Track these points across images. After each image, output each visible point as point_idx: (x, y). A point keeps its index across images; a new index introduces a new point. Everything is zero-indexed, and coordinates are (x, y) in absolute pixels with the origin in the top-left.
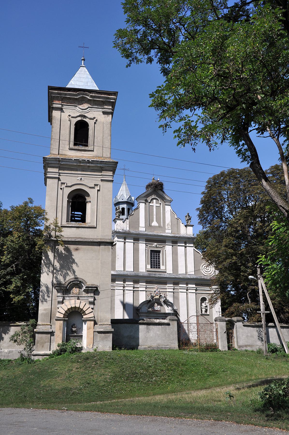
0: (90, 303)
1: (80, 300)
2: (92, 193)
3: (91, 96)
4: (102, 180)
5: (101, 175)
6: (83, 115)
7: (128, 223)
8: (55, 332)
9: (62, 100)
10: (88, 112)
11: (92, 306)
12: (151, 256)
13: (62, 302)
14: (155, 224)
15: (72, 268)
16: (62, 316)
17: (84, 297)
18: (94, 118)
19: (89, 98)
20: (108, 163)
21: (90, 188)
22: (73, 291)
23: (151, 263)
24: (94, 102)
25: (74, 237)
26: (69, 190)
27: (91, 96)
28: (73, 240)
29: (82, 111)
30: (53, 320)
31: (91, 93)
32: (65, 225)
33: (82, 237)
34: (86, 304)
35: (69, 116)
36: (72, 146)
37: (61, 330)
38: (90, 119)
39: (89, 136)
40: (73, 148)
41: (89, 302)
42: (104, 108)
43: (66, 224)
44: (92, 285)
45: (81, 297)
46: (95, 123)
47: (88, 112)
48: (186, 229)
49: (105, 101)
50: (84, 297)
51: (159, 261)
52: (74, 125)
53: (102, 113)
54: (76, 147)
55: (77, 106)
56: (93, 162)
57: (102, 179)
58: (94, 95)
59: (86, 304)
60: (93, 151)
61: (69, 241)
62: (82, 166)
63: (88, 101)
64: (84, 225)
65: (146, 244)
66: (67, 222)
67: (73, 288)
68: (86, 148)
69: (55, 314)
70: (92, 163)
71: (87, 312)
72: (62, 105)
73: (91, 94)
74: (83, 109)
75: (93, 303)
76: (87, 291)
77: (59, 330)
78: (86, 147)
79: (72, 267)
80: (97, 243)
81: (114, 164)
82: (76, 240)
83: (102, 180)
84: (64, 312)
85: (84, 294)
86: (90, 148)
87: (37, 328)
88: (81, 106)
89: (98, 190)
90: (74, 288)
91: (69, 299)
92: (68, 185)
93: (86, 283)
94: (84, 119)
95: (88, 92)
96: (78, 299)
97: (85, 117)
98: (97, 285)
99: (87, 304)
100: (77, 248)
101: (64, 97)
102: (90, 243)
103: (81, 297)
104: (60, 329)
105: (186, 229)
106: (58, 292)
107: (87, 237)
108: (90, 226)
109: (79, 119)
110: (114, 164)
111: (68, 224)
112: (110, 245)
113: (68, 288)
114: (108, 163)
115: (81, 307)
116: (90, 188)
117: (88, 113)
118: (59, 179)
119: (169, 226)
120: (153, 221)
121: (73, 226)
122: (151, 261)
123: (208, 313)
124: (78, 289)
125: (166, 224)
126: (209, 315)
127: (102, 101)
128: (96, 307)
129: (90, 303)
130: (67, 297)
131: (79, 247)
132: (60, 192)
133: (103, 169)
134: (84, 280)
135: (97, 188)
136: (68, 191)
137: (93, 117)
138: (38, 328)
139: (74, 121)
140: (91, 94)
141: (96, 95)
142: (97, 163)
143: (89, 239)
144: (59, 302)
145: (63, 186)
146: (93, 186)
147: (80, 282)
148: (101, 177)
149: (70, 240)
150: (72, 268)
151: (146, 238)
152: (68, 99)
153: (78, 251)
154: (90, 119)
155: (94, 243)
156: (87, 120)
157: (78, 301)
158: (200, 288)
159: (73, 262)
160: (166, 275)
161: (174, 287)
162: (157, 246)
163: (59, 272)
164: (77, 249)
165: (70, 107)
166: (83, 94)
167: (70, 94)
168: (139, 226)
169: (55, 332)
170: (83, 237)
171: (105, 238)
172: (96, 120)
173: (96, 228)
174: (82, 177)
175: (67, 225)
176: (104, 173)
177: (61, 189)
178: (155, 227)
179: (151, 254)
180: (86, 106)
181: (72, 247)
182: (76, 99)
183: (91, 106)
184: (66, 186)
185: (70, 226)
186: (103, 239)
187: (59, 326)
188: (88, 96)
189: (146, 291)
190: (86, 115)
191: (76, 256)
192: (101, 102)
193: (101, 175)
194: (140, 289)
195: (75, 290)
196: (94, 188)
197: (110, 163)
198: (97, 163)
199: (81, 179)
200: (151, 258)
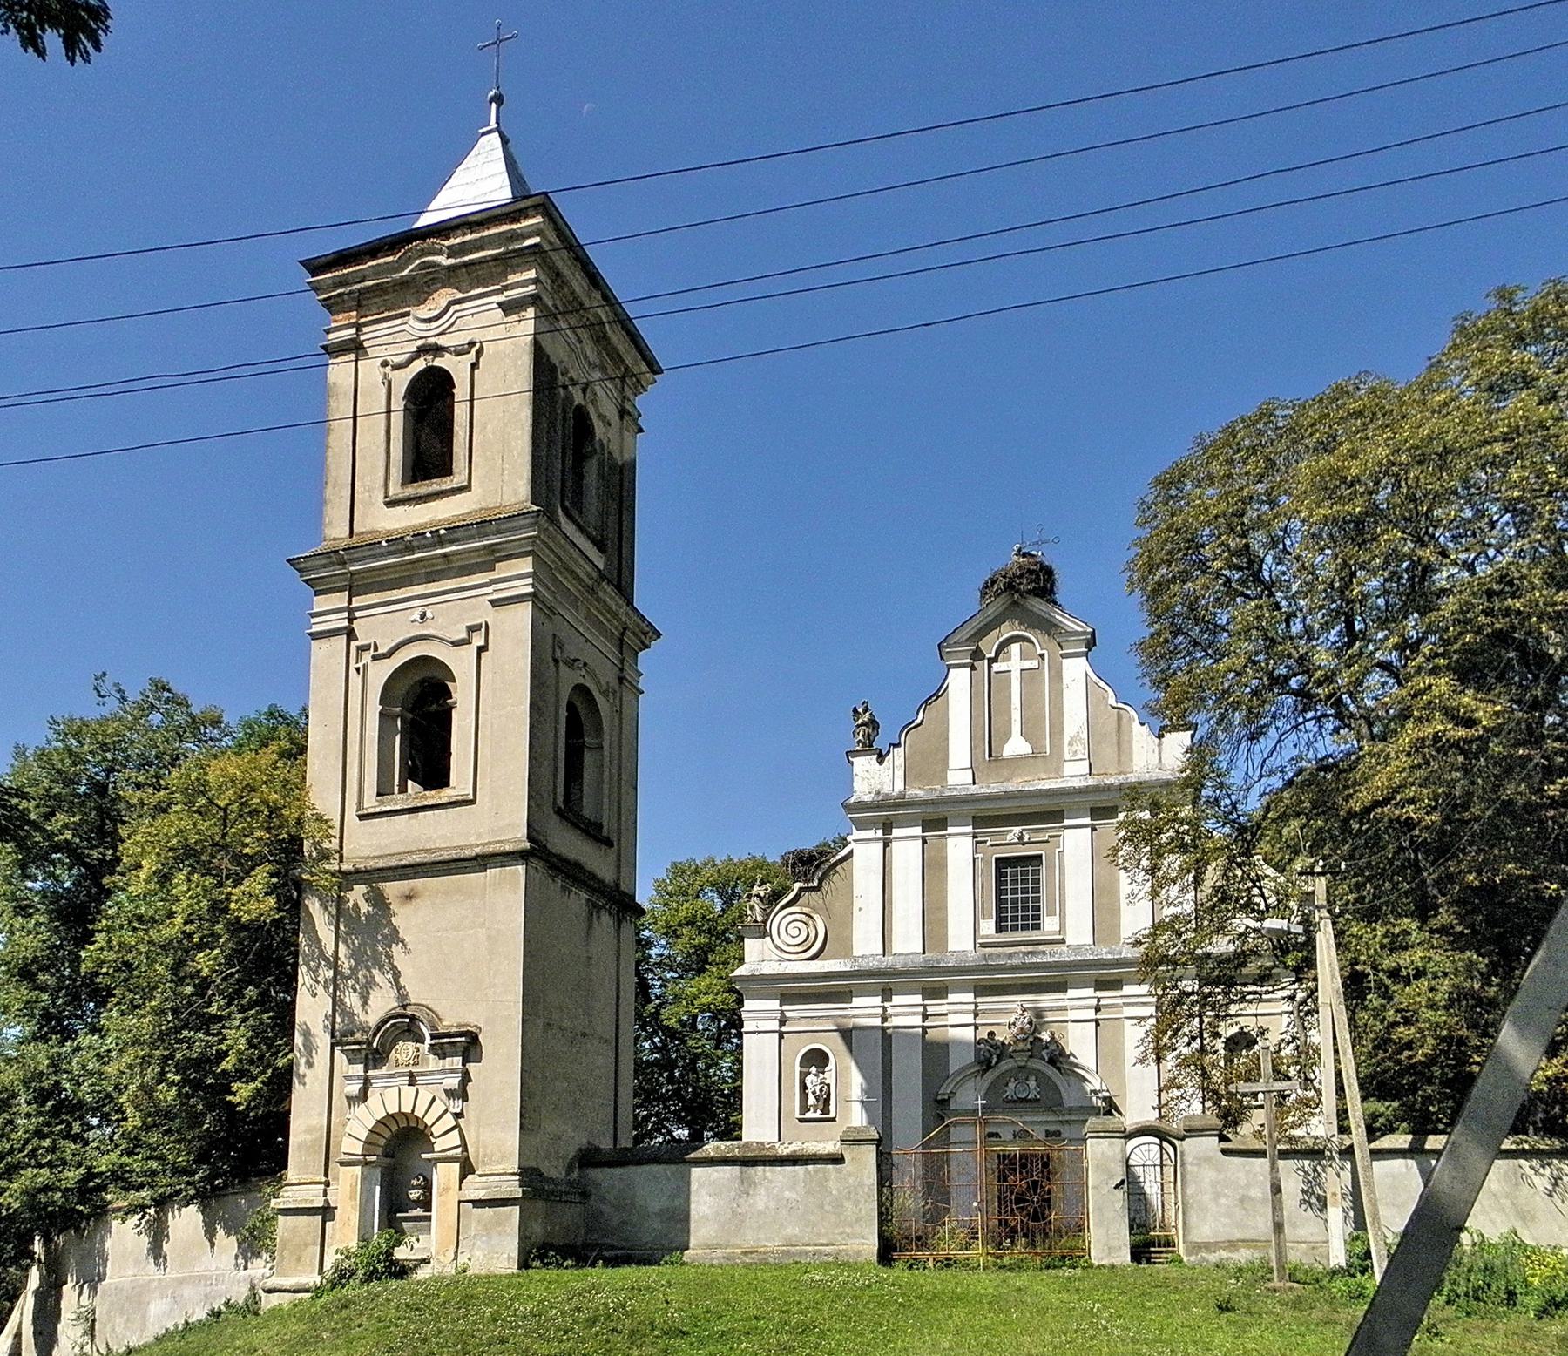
1: (414, 1088)
2: (460, 663)
3: (453, 252)
4: (495, 603)
5: (493, 582)
7: (900, 761)
11: (456, 1106)
13: (363, 1096)
14: (1016, 746)
16: (358, 1148)
17: (432, 1073)
19: (443, 260)
21: (455, 644)
27: (453, 252)
31: (448, 238)
32: (372, 811)
34: (434, 1099)
36: (395, 490)
39: (456, 427)
42: (506, 288)
44: (459, 1025)
45: (422, 1074)
46: (474, 366)
48: (1160, 745)
49: (504, 254)
52: (404, 398)
54: (412, 490)
55: (408, 314)
56: (455, 535)
57: (495, 596)
58: (458, 240)
59: (434, 1099)
60: (466, 488)
62: (426, 563)
63: (450, 277)
66: (379, 794)
68: (446, 483)
70: (452, 542)
72: (359, 327)
74: (429, 321)
76: (440, 1051)
81: (531, 525)
82: (403, 862)
83: (495, 603)
84: (363, 1135)
85: (433, 1063)
86: (458, 479)
88: (425, 311)
90: (401, 1043)
92: (380, 651)
94: (438, 362)
96: (412, 1082)
97: (437, 350)
99: (437, 1100)
103: (422, 1074)
105: (1160, 745)
106: (351, 1062)
108: (454, 799)
109: (419, 365)
110: (531, 525)
111: (382, 803)
113: (375, 1045)
115: (419, 1113)
116: (455, 644)
118: (350, 634)
119: (1081, 748)
120: (1007, 735)
121: (398, 807)
124: (411, 1046)
125: (1067, 739)
127: (495, 258)
130: (376, 1077)
132: (355, 680)
135: (478, 640)
136: (380, 673)
139: (402, 379)
141: (468, 237)
144: (351, 1100)
145: (367, 657)
146: (464, 635)
148: (490, 590)
149: (381, 864)
154: (459, 353)
156: (444, 362)
164: (409, 897)
165: (385, 325)
166: (424, 253)
172: (479, 353)
173: (473, 802)
175: (378, 810)
176: (504, 569)
177: (358, 670)
178: (1017, 760)
180: (442, 297)
181: (392, 889)
182: (404, 284)
183: (461, 295)
184: (374, 658)
185: (388, 808)
188: (440, 253)
190: (442, 341)
191: (402, 918)
193: (493, 582)
195: (404, 1050)
196: (466, 642)
199: (423, 616)
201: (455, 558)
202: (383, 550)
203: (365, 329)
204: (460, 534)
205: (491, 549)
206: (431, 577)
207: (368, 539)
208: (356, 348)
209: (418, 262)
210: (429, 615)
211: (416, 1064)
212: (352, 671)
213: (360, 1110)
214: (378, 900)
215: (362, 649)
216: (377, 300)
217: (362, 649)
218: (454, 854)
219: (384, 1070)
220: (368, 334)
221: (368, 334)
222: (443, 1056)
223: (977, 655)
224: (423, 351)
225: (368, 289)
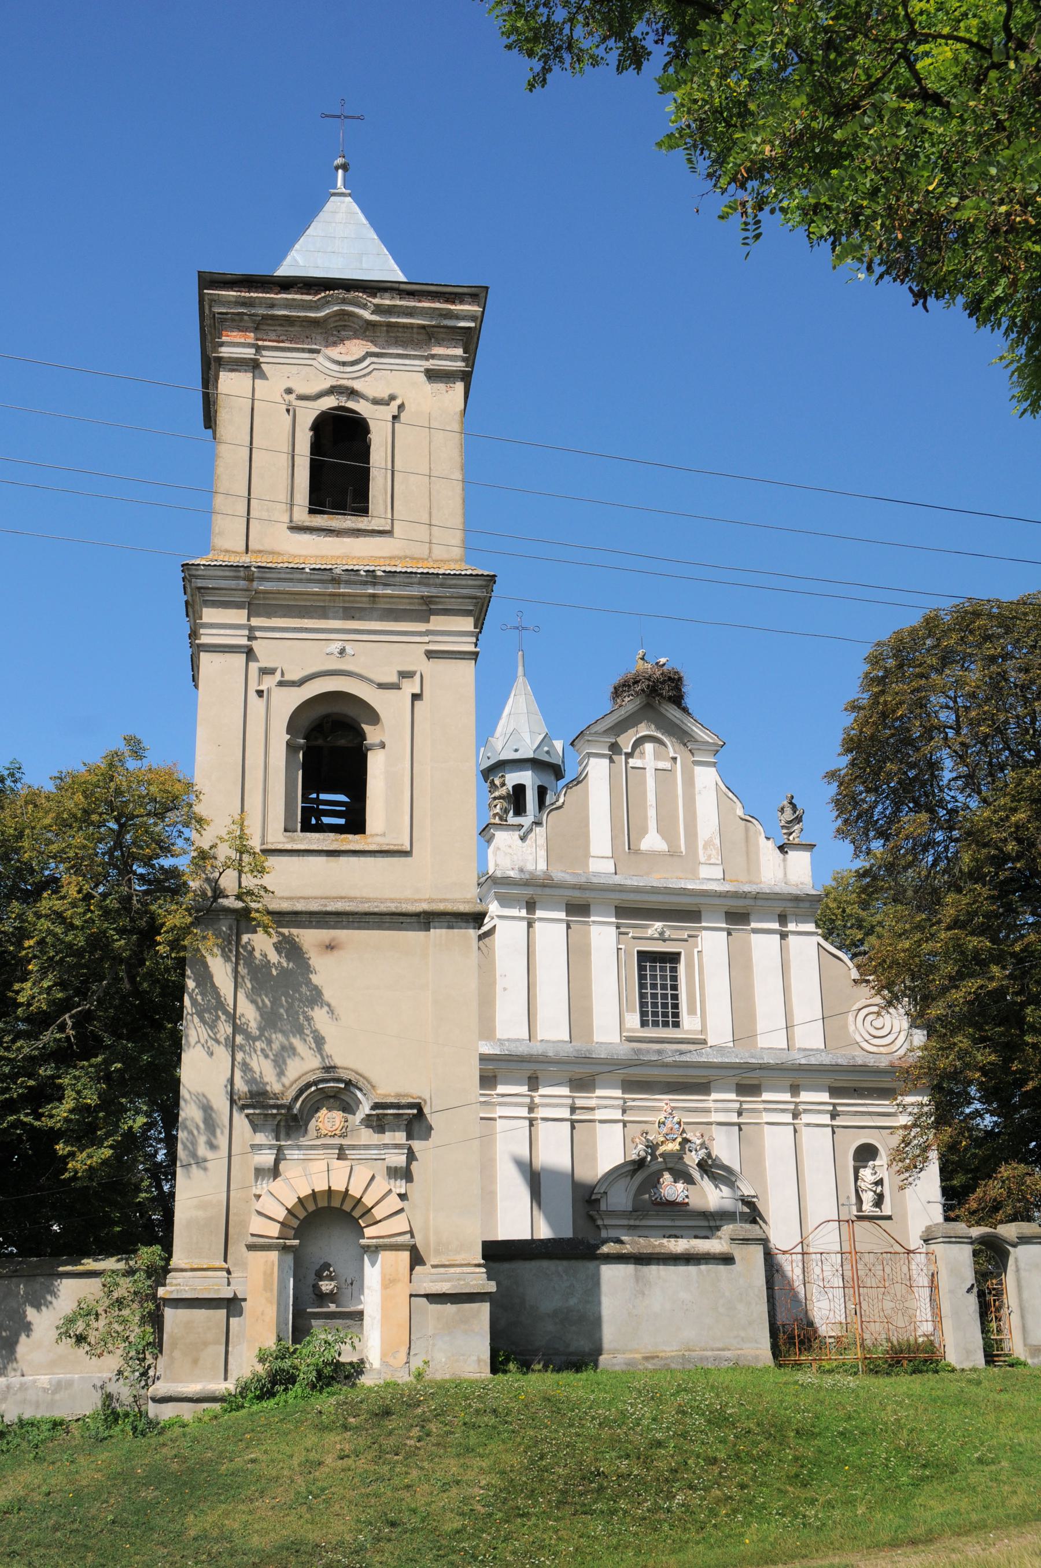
0: (394, 1173)
1: (348, 1163)
3: (378, 310)
4: (430, 655)
5: (428, 633)
6: (347, 388)
8: (245, 1300)
9: (256, 329)
10: (364, 376)
11: (400, 1186)
12: (642, 977)
15: (309, 1024)
17: (367, 1147)
18: (392, 398)
19: (367, 315)
20: (454, 582)
21: (382, 686)
22: (320, 1125)
23: (643, 1005)
24: (388, 331)
25: (318, 893)
26: (293, 699)
27: (378, 310)
28: (314, 907)
29: (342, 369)
30: (237, 1249)
31: (374, 296)
32: (280, 847)
33: (352, 893)
34: (373, 1178)
35: (289, 391)
36: (302, 515)
37: (272, 1290)
38: (376, 402)
40: (307, 524)
41: (389, 1169)
42: (433, 357)
43: (284, 840)
44: (398, 1095)
45: (354, 1147)
47: (364, 376)
49: (433, 326)
50: (367, 1147)
51: (675, 997)
53: (422, 378)
54: (320, 521)
55: (318, 351)
59: (373, 1178)
61: (296, 913)
62: (347, 598)
63: (367, 331)
64: (357, 842)
65: (618, 928)
66: (286, 830)
67: (317, 1110)
68: (362, 523)
69: (245, 1224)
71: (378, 1213)
72: (258, 349)
73: (376, 301)
74: (344, 364)
75: (405, 1174)
76: (377, 1122)
77: (265, 1290)
78: (360, 519)
79: (309, 1019)
80: (414, 919)
81: (480, 587)
83: (430, 655)
84: (281, 1214)
85: (367, 1136)
87: (171, 1285)
88: (334, 352)
89: (416, 697)
91: (302, 1157)
92: (287, 678)
93: (373, 1087)
94: (351, 405)
95: (364, 292)
96: (341, 1157)
97: (352, 393)
98: (420, 1098)
100: (333, 939)
101: (265, 317)
102: (387, 919)
103: (354, 1147)
104: (267, 1287)
106: (255, 1128)
107: (371, 896)
109: (329, 403)
111: (293, 840)
112: (472, 925)
113: (295, 1111)
114: (454, 582)
116: (382, 686)
117: (367, 378)
122: (642, 996)
123: (887, 1210)
124: (338, 1116)
126: (889, 1218)
128: (415, 1190)
129: (394, 1173)
130: (291, 1147)
131: (341, 935)
133: (433, 607)
134: (366, 1074)
135: (411, 687)
137: (385, 396)
138: (174, 1281)
139: (308, 413)
140: (376, 301)
142: (406, 580)
143: (382, 901)
145: (269, 683)
146: (394, 678)
147: (349, 1083)
148: (426, 639)
149: (300, 907)
150: (309, 1024)
151: (617, 903)
152: (281, 325)
153: (335, 953)
154: (376, 402)
155: (402, 919)
156: (361, 407)
157: (341, 1168)
158: (847, 1104)
159: (316, 997)
160: (707, 1056)
161: (741, 1102)
162: (667, 935)
163: (257, 1044)
164: (330, 947)
165: (289, 354)
166: (344, 301)
167: (289, 305)
168: (587, 855)
169: (245, 1300)
170: (358, 895)
171: (448, 896)
172: (401, 407)
173: (407, 854)
174: (345, 644)
175: (289, 847)
176: (438, 623)
179: (641, 968)
180: (355, 348)
181: (308, 938)
182: (315, 323)
186: (441, 901)
187: (265, 1273)
188: (364, 307)
189: (625, 1124)
190: (357, 385)
192: (418, 333)
193: (428, 633)
194: (599, 1115)
195: (328, 1119)
196: (396, 687)
197: (464, 582)
198: (409, 580)
199: (342, 651)
200: (642, 986)
201: (381, 600)
202: (304, 576)
203: (264, 353)
204: (398, 579)
205: (427, 600)
206: (350, 613)
207: (264, 561)
208: (254, 366)
209: (335, 308)
210: (349, 650)
211: (343, 1136)
212: (252, 695)
213: (276, 1186)
214: (291, 949)
215: (265, 671)
216: (279, 328)
217: (265, 671)
218: (392, 907)
219: (304, 1141)
220: (266, 357)
221: (266, 357)
222: (380, 1129)
223: (615, 748)
224: (332, 391)
225: (274, 317)
